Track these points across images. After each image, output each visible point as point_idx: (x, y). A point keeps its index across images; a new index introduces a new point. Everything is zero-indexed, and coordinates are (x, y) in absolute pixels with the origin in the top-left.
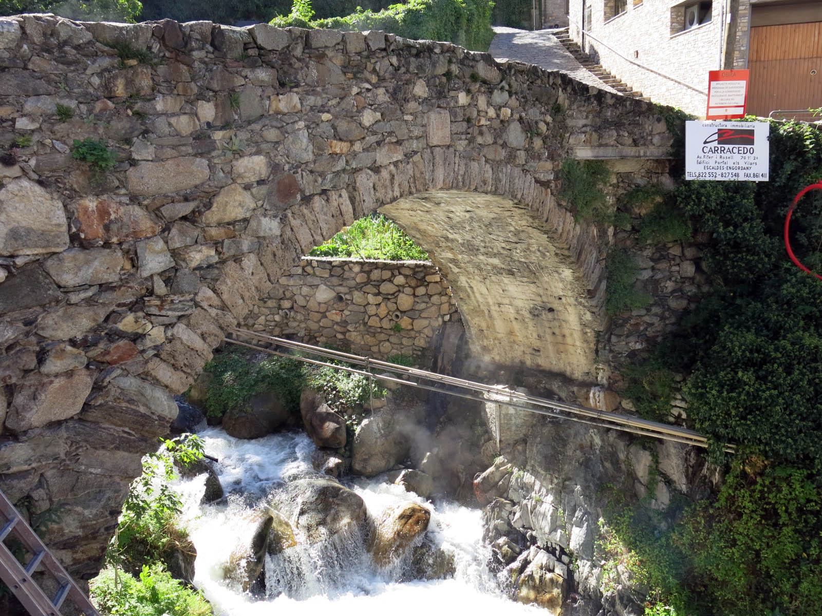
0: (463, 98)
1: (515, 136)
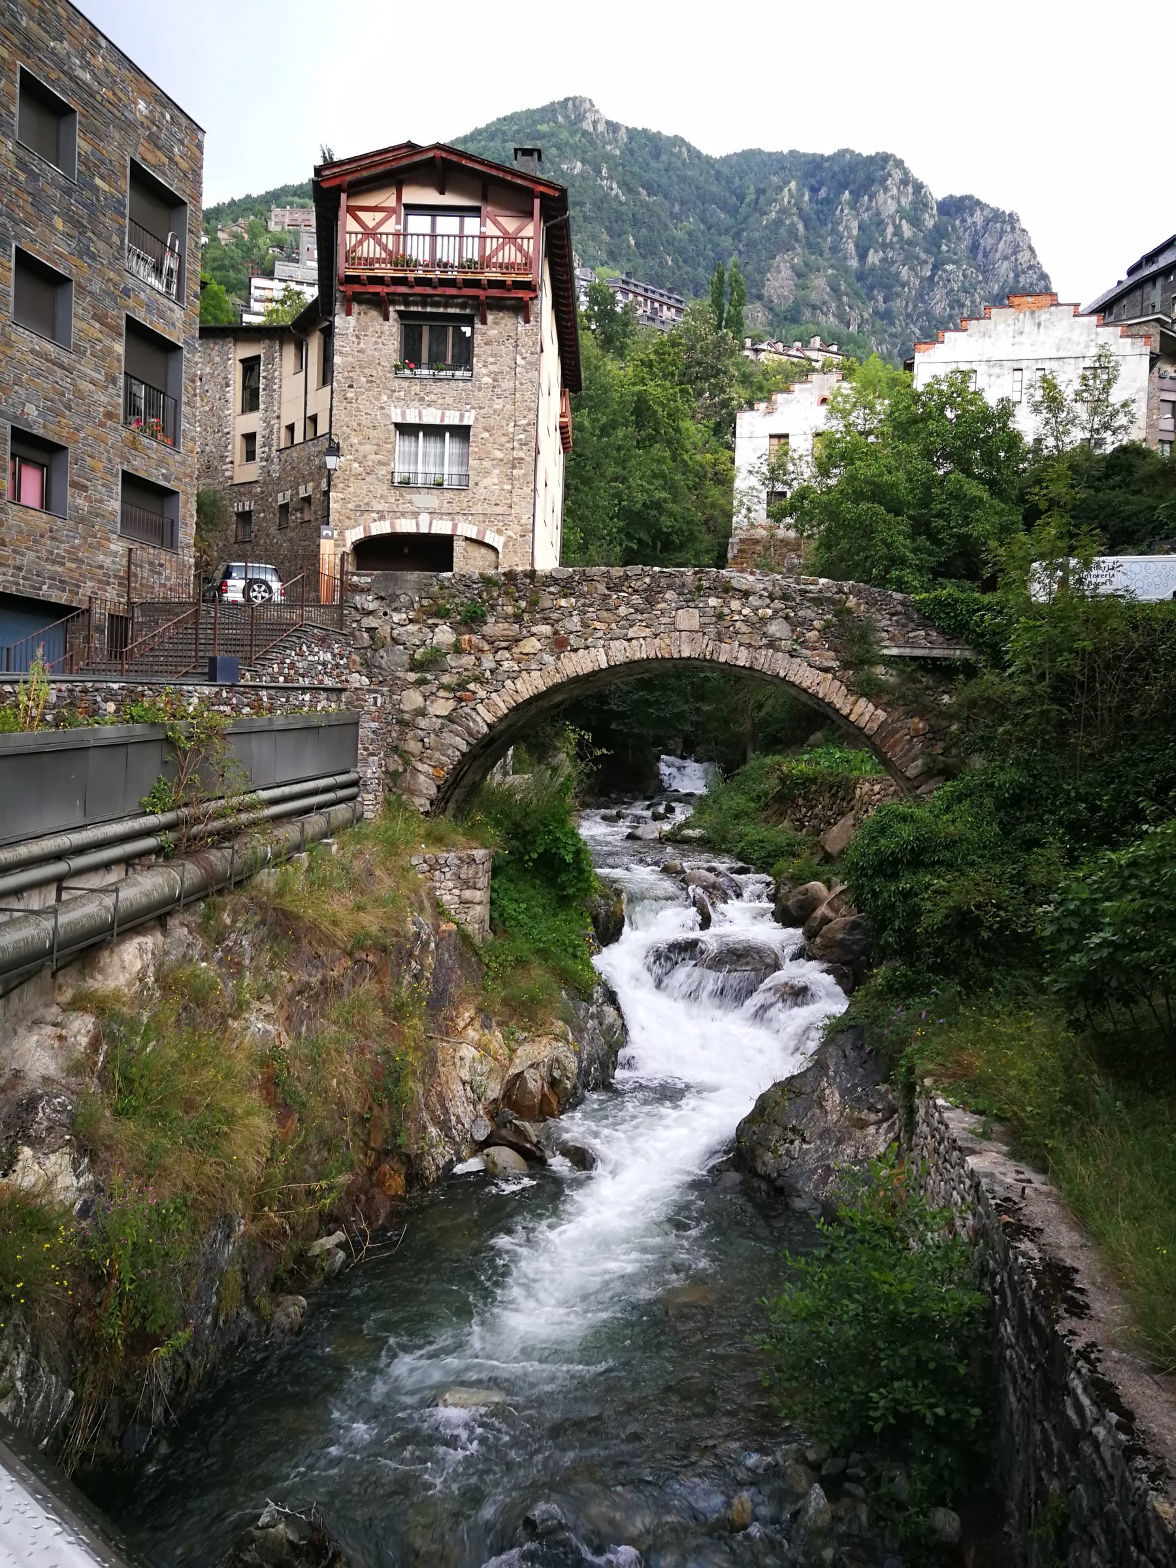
0: (713, 601)
1: (777, 628)
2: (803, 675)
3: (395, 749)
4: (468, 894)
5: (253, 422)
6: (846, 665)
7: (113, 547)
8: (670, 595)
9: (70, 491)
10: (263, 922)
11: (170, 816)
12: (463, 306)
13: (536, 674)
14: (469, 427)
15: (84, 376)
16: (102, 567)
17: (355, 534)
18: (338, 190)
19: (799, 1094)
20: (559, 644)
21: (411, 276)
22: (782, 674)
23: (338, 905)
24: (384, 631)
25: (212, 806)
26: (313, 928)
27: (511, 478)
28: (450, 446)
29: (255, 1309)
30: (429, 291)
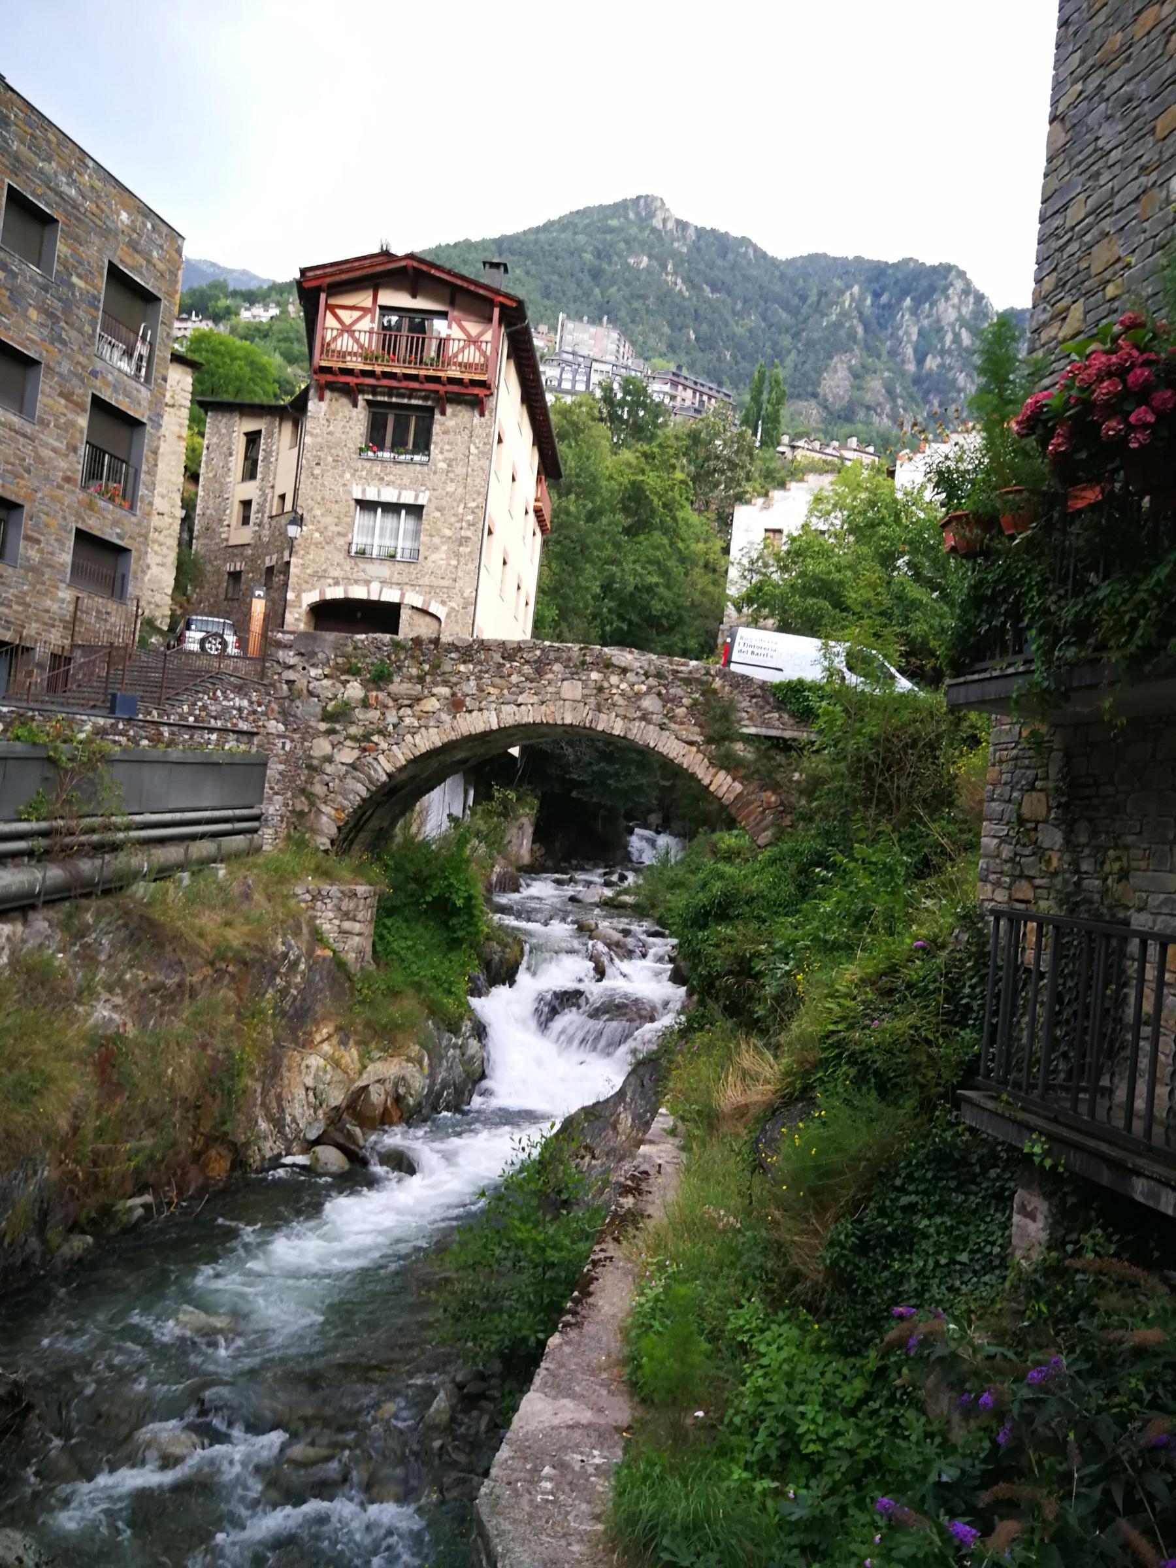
0: (595, 675)
1: (650, 703)
2: (671, 747)
3: (303, 791)
4: (347, 925)
5: (250, 491)
6: (709, 740)
7: (61, 595)
8: (557, 667)
9: (22, 543)
10: (126, 926)
11: (44, 825)
12: (425, 398)
13: (433, 731)
14: (422, 507)
15: (45, 445)
16: (47, 611)
17: (311, 597)
18: (318, 290)
19: (598, 1117)
20: (456, 705)
21: (378, 369)
22: (652, 745)
23: (209, 921)
24: (301, 684)
25: (97, 821)
26: (177, 937)
27: (458, 555)
28: (405, 522)
29: (44, 1241)
30: (394, 383)
